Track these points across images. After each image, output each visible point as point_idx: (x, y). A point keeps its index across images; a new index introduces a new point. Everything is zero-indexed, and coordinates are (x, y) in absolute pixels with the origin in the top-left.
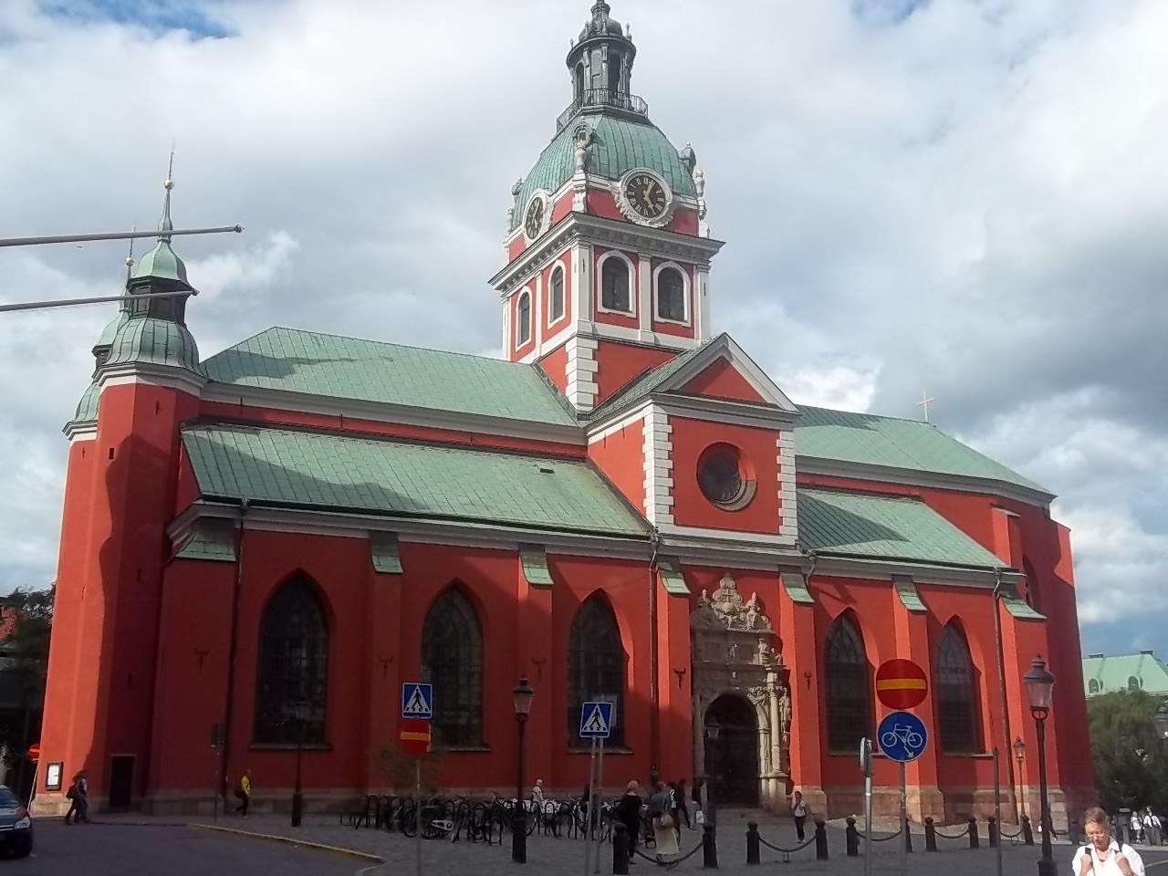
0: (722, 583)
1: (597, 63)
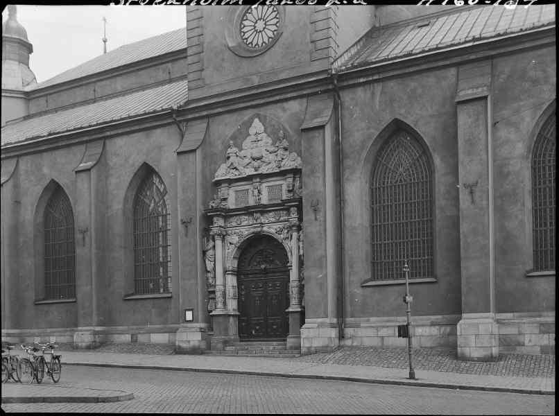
0: (252, 131)
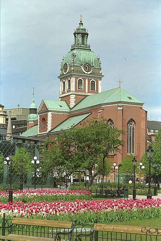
1: (79, 38)
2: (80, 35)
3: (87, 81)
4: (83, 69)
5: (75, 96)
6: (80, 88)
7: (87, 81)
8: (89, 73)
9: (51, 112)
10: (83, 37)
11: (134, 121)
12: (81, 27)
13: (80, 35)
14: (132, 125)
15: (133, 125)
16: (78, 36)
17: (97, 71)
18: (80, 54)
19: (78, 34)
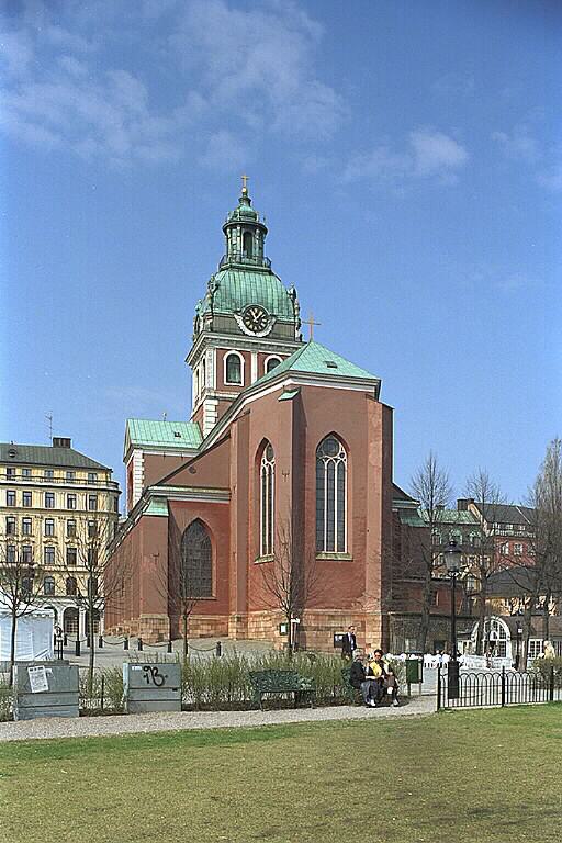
1: (237, 239)
2: (239, 228)
3: (254, 359)
4: (241, 324)
5: (216, 402)
6: (232, 379)
7: (254, 359)
8: (260, 335)
9: (141, 452)
10: (247, 237)
11: (341, 440)
12: (245, 208)
13: (239, 228)
14: (338, 457)
15: (342, 456)
16: (234, 234)
17: (285, 331)
18: (232, 281)
19: (233, 226)
